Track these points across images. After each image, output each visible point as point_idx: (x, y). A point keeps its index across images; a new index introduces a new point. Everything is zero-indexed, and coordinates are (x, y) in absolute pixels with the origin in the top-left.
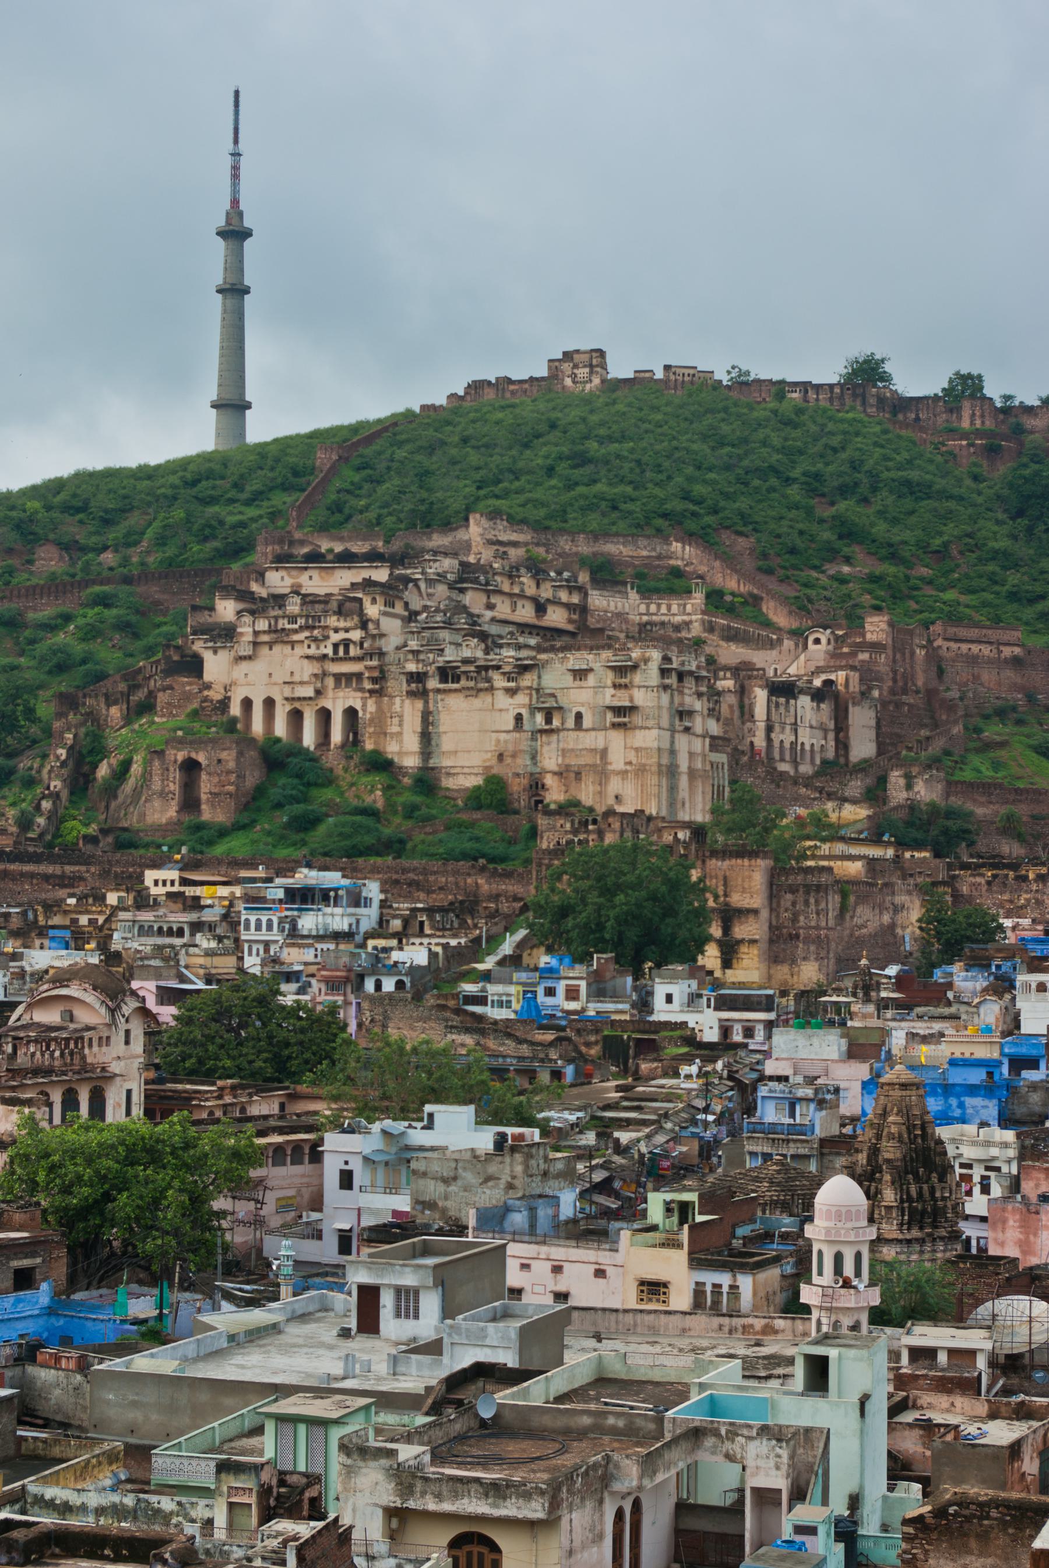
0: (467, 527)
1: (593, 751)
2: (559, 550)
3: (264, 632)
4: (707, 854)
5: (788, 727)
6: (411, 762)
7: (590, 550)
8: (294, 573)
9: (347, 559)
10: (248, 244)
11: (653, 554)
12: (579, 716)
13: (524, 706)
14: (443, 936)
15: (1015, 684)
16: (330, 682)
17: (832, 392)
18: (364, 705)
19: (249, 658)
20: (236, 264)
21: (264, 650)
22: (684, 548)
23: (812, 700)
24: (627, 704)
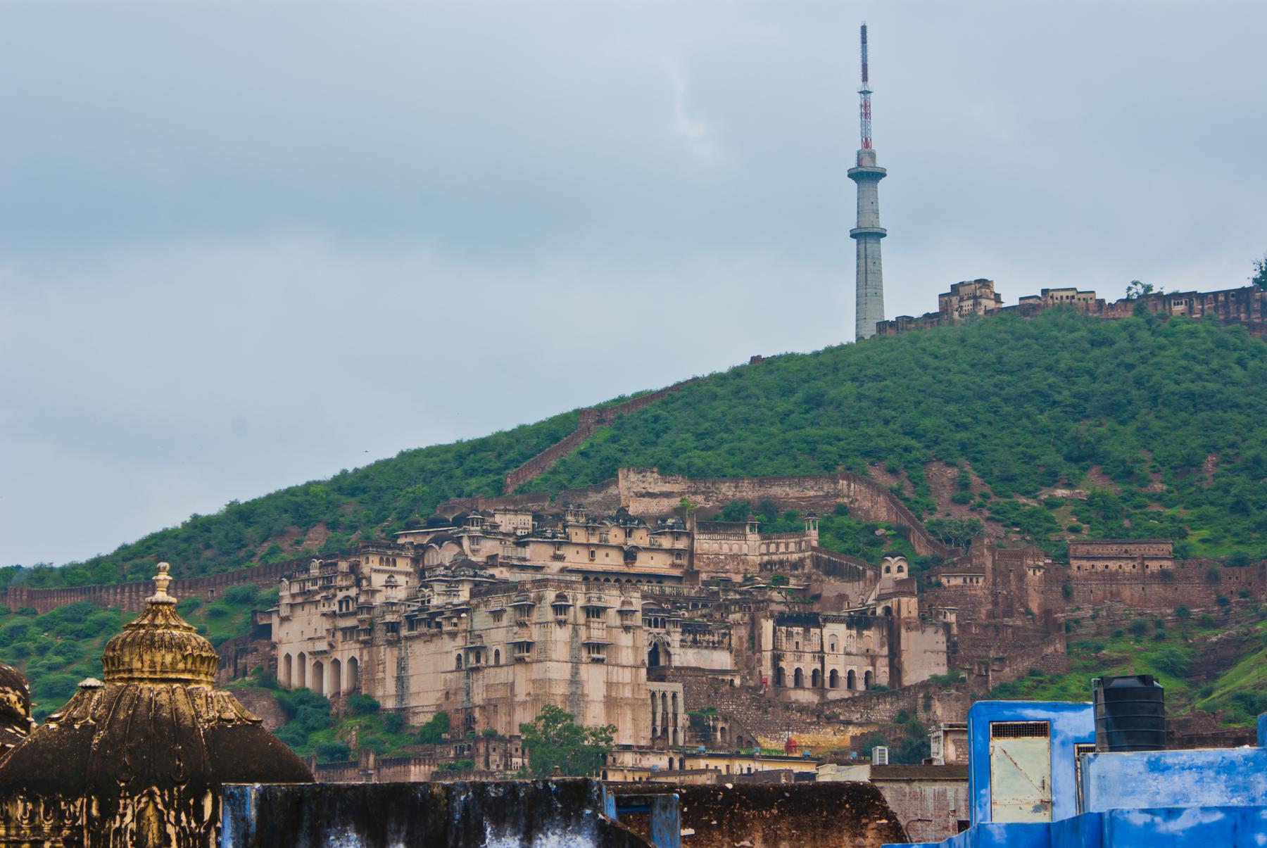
0: (616, 483)
1: (505, 684)
2: (721, 497)
5: (808, 657)
6: (390, 704)
7: (756, 494)
10: (882, 184)
11: (821, 493)
12: (497, 653)
15: (1165, 599)
16: (339, 635)
17: (1216, 301)
18: (361, 655)
20: (866, 206)
21: (299, 611)
22: (849, 485)
23: (849, 627)
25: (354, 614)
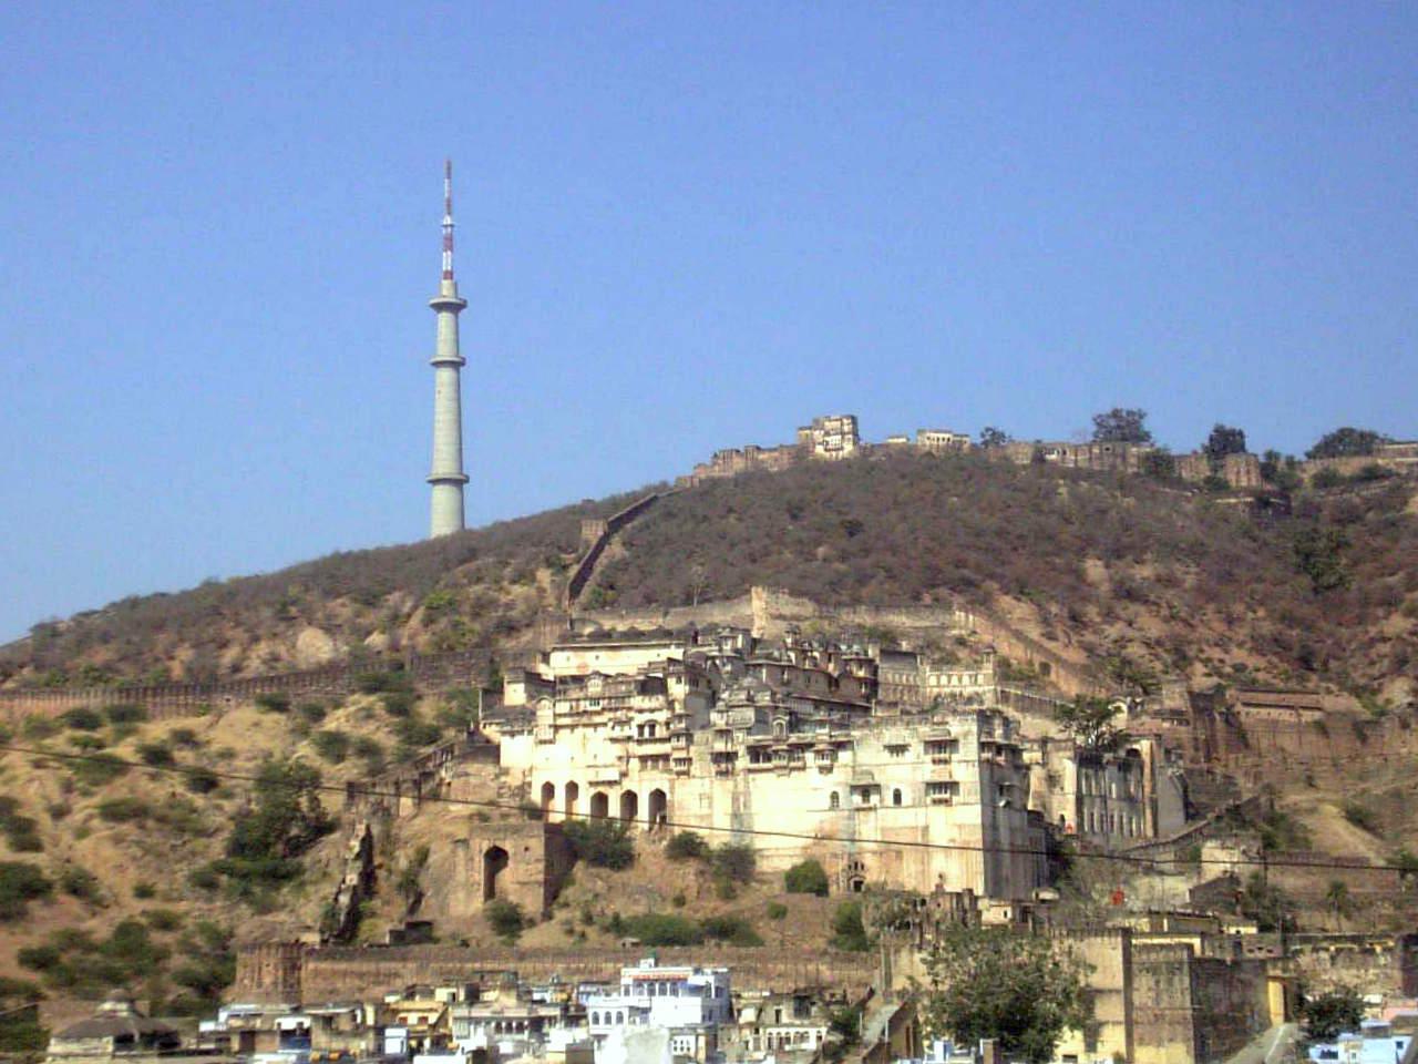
0: (750, 600)
1: (914, 828)
2: (842, 623)
3: (565, 715)
4: (1065, 933)
8: (581, 653)
9: (635, 639)
11: (936, 624)
12: (897, 797)
13: (839, 784)
14: (802, 1026)
16: (635, 764)
19: (551, 742)
21: (564, 733)
22: (967, 617)
23: (1120, 769)
24: (947, 779)
25: (668, 740)
